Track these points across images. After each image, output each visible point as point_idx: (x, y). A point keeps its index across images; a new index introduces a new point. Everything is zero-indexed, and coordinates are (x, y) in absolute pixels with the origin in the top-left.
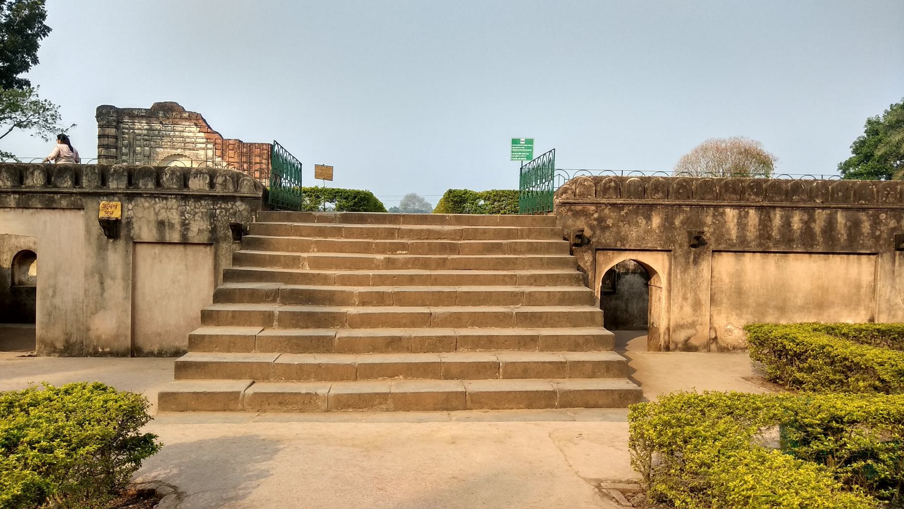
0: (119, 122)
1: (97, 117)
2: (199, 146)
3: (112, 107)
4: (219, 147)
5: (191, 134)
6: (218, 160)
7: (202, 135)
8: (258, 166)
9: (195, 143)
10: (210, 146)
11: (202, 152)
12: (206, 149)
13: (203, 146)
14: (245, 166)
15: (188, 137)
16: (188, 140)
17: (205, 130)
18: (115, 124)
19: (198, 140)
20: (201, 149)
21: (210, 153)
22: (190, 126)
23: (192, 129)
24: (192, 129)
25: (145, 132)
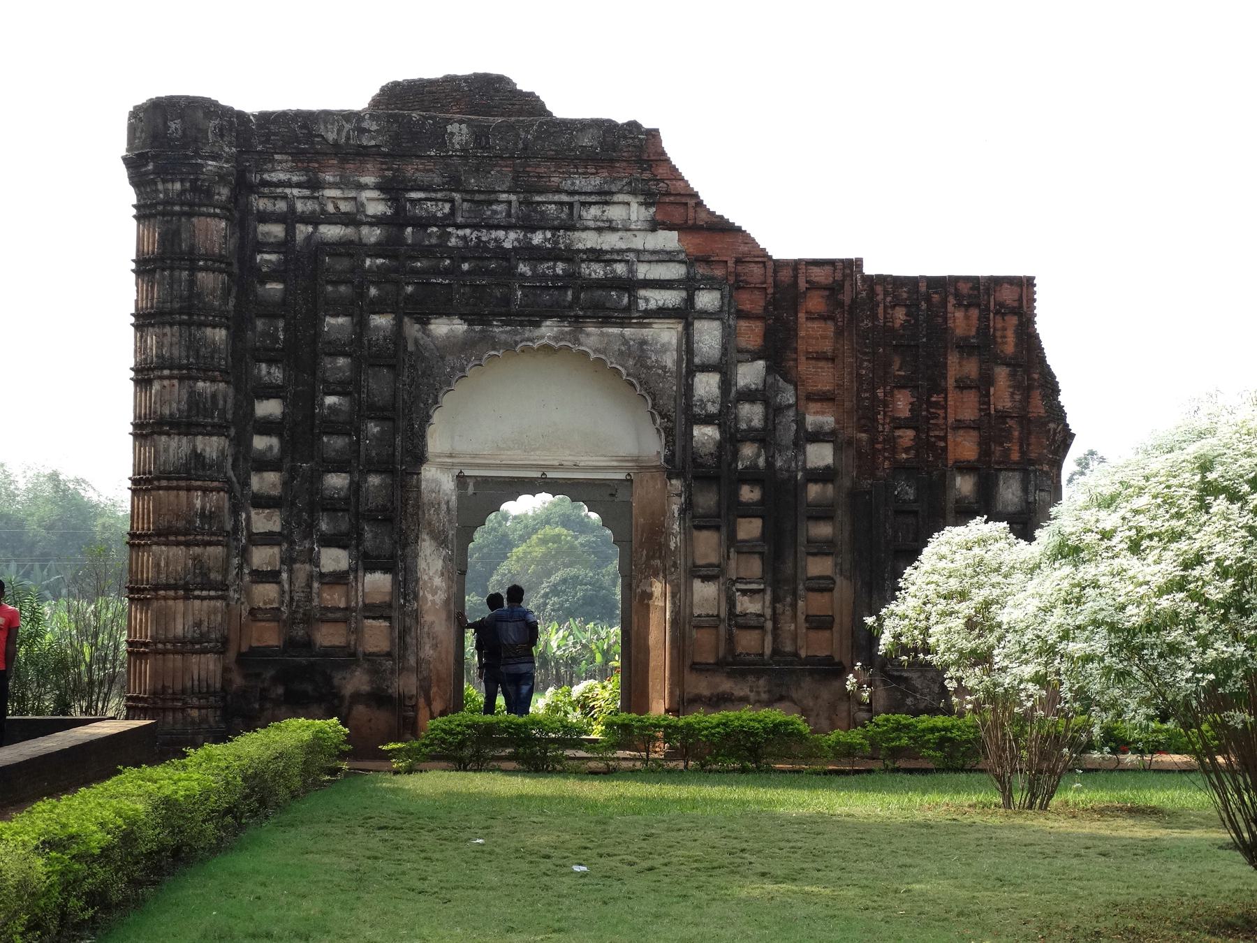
0: (243, 187)
1: (134, 163)
2: (656, 298)
3: (207, 107)
4: (751, 302)
5: (610, 241)
6: (750, 374)
7: (668, 240)
8: (965, 407)
9: (631, 285)
10: (707, 299)
11: (666, 334)
12: (685, 314)
13: (671, 298)
14: (903, 403)
15: (596, 255)
16: (597, 271)
17: (677, 215)
18: (224, 193)
19: (643, 271)
20: (663, 313)
21: (709, 337)
22: (604, 197)
23: (615, 213)
24: (615, 213)
25: (372, 235)
